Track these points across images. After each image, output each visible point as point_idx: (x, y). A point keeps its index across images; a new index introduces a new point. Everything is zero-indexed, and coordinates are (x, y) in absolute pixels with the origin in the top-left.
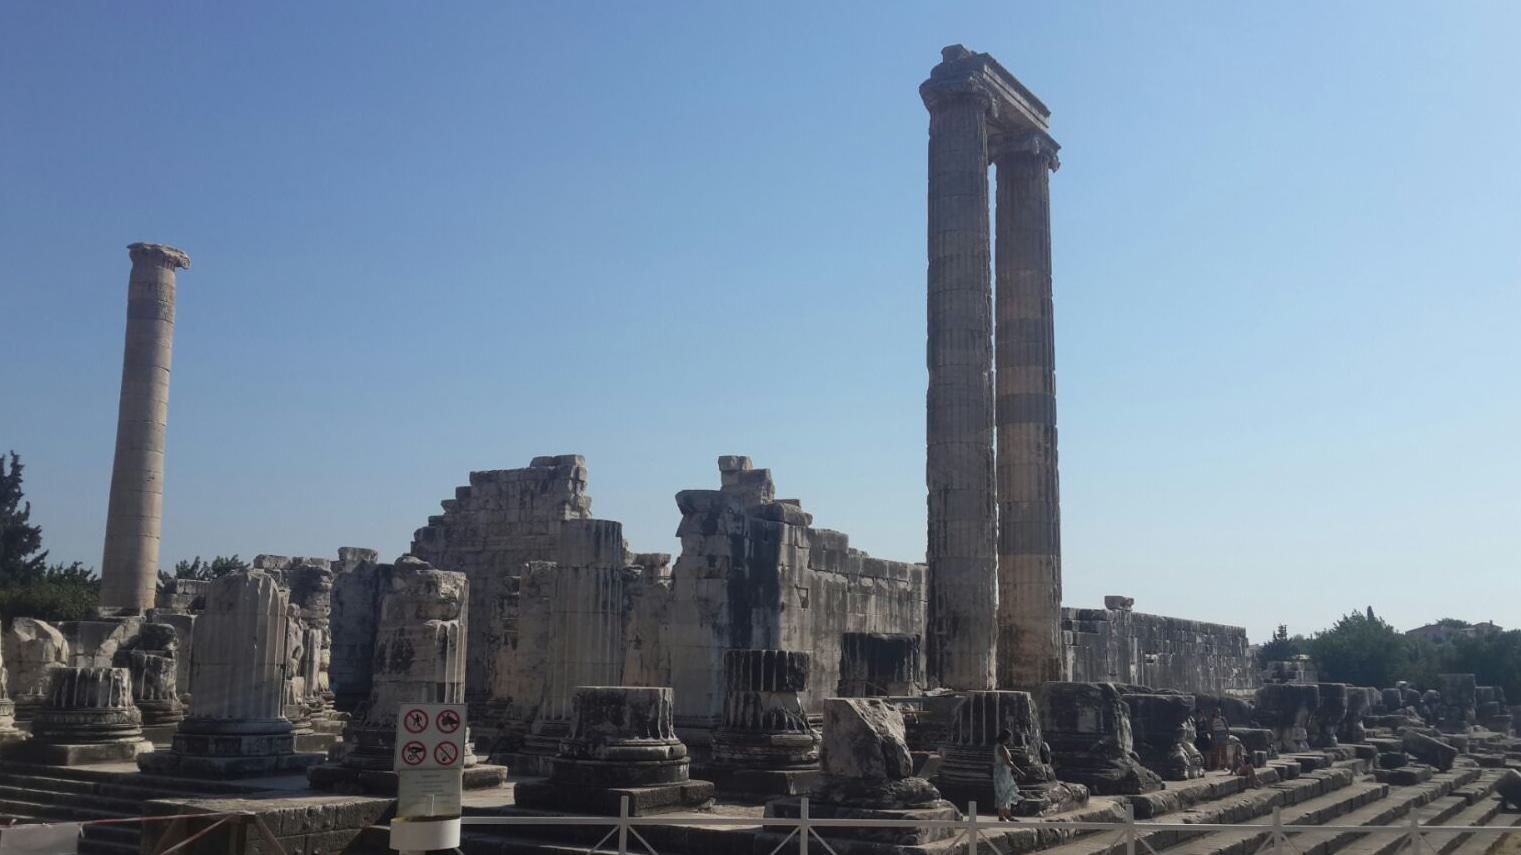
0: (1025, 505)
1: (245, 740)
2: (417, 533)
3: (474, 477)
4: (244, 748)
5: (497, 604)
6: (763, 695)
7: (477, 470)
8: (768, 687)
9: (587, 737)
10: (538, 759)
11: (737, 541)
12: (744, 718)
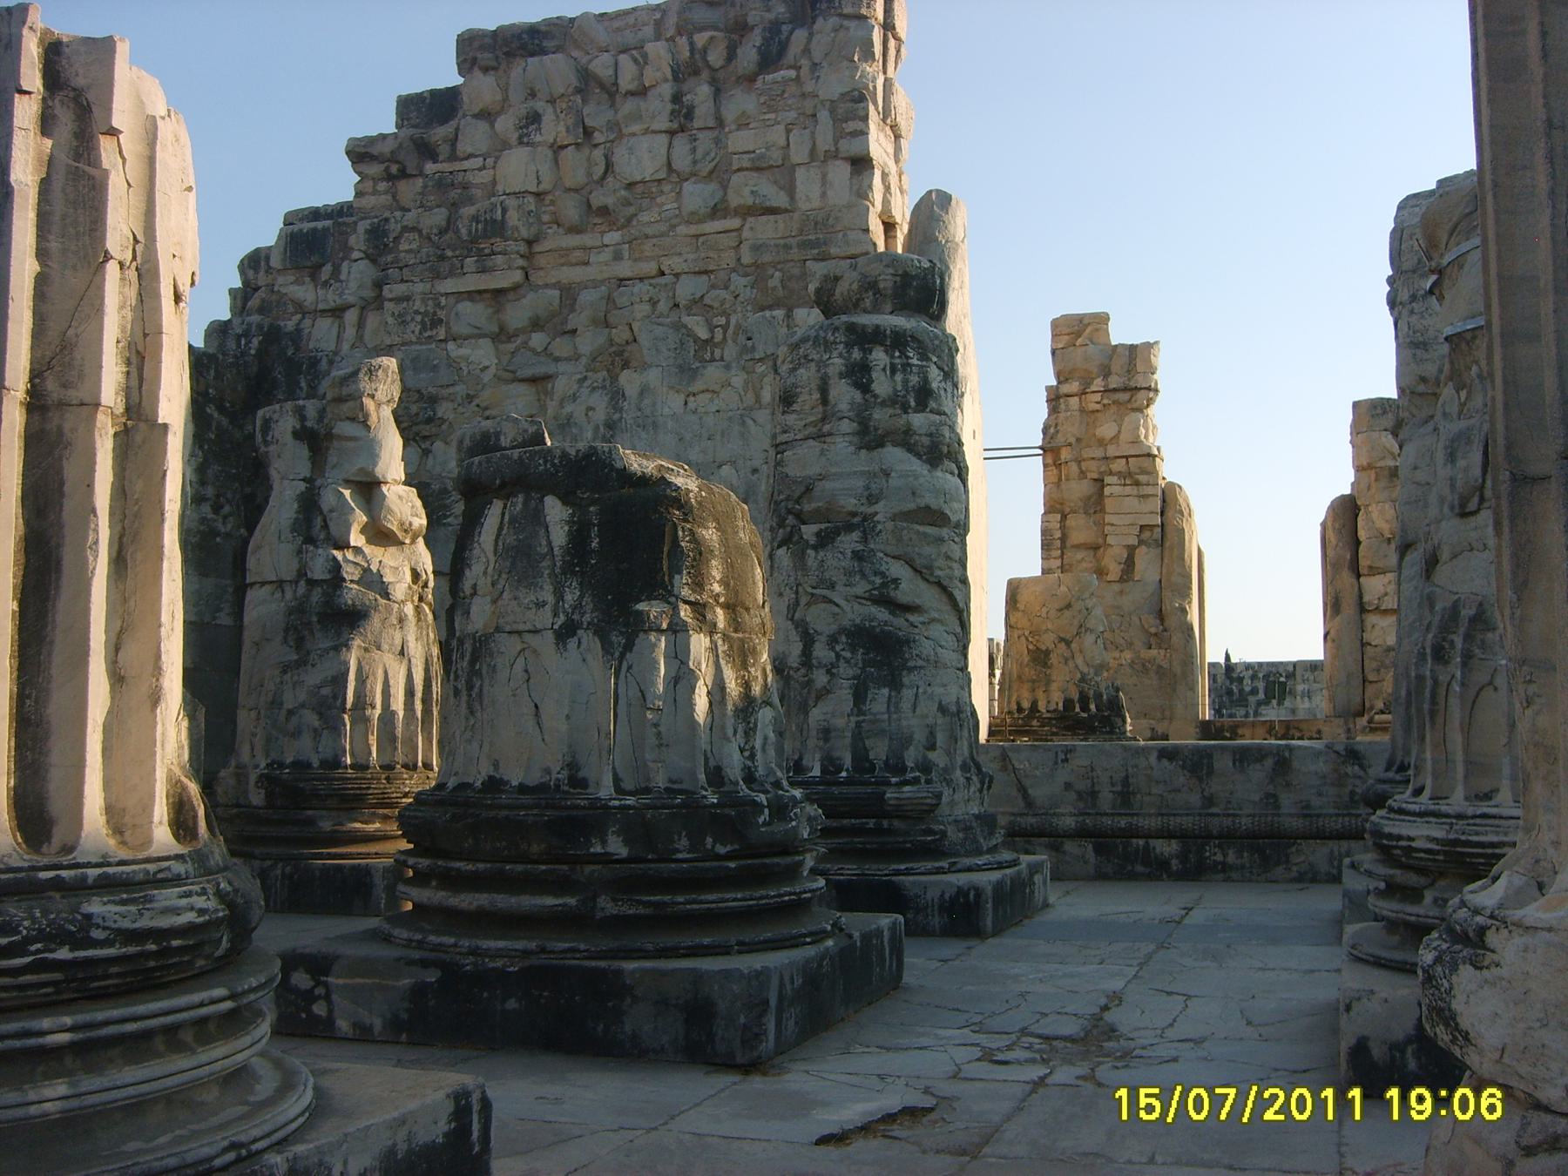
3: (477, 50)
5: (837, 363)
7: (489, 22)
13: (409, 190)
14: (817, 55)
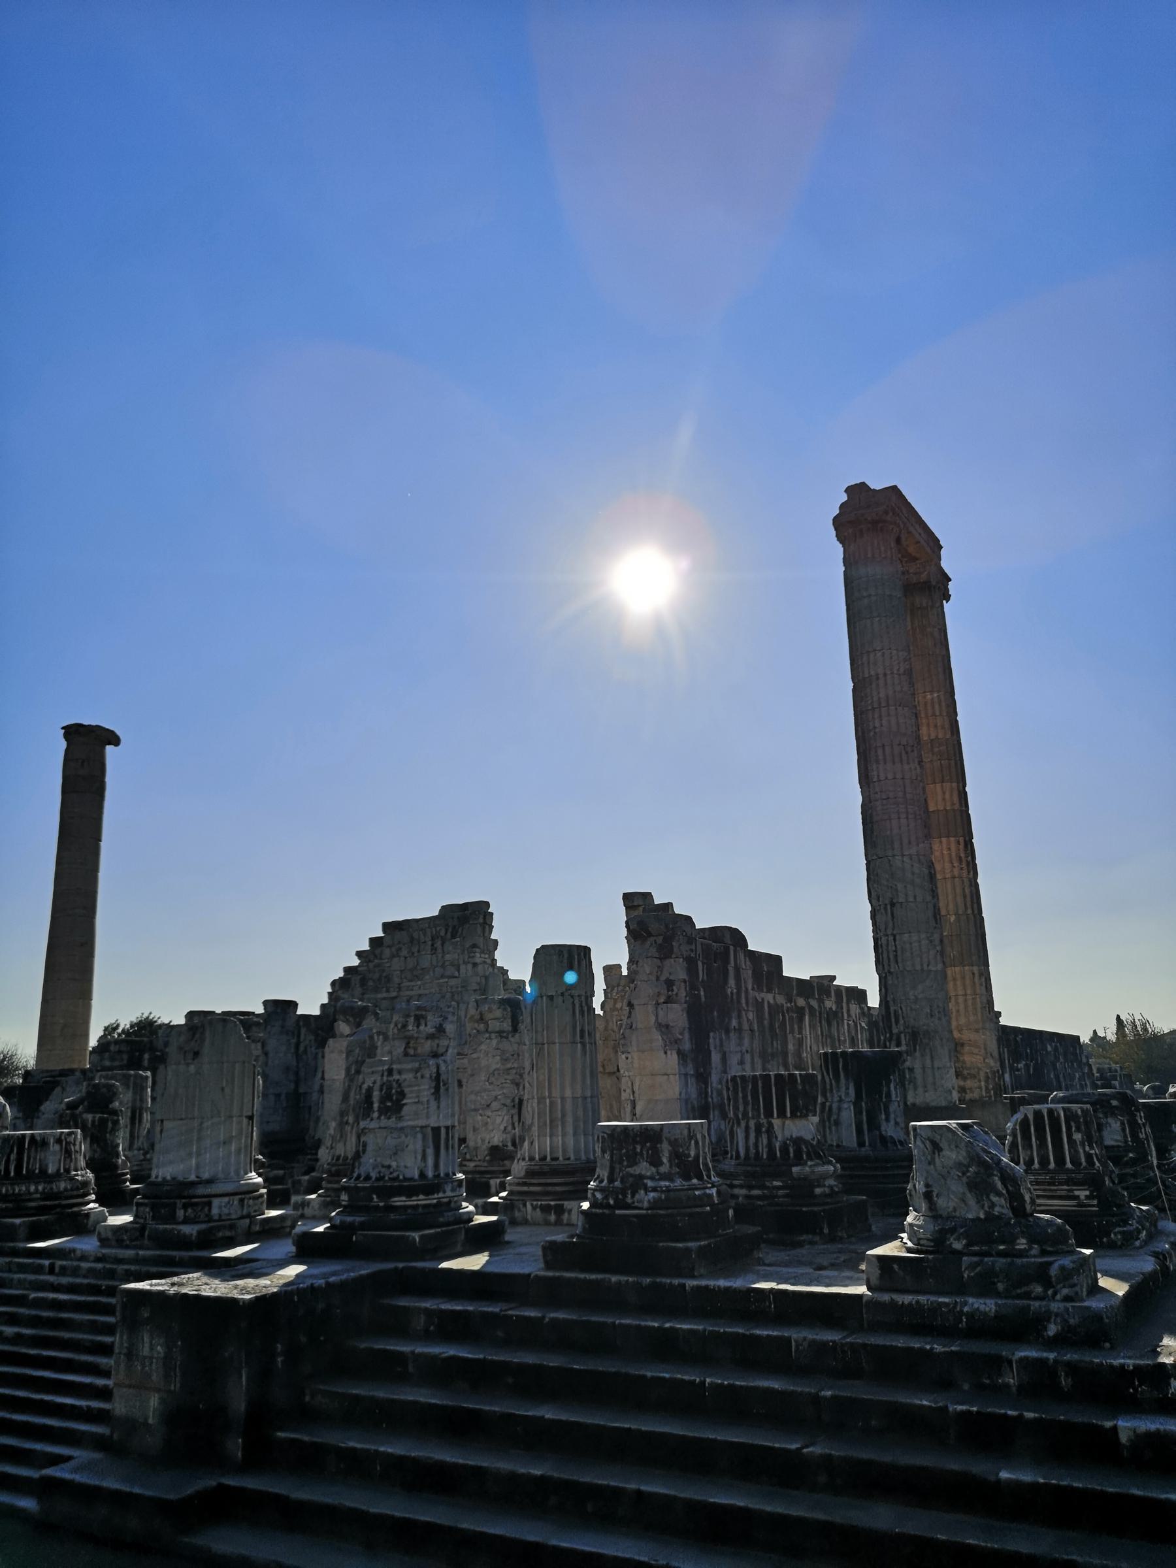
0: (953, 918)
1: (216, 1202)
2: (333, 984)
3: (386, 926)
4: (215, 1211)
6: (776, 1122)
8: (782, 1114)
9: (622, 1182)
10: (525, 1205)
11: (691, 963)
12: (757, 1153)
13: (371, 965)
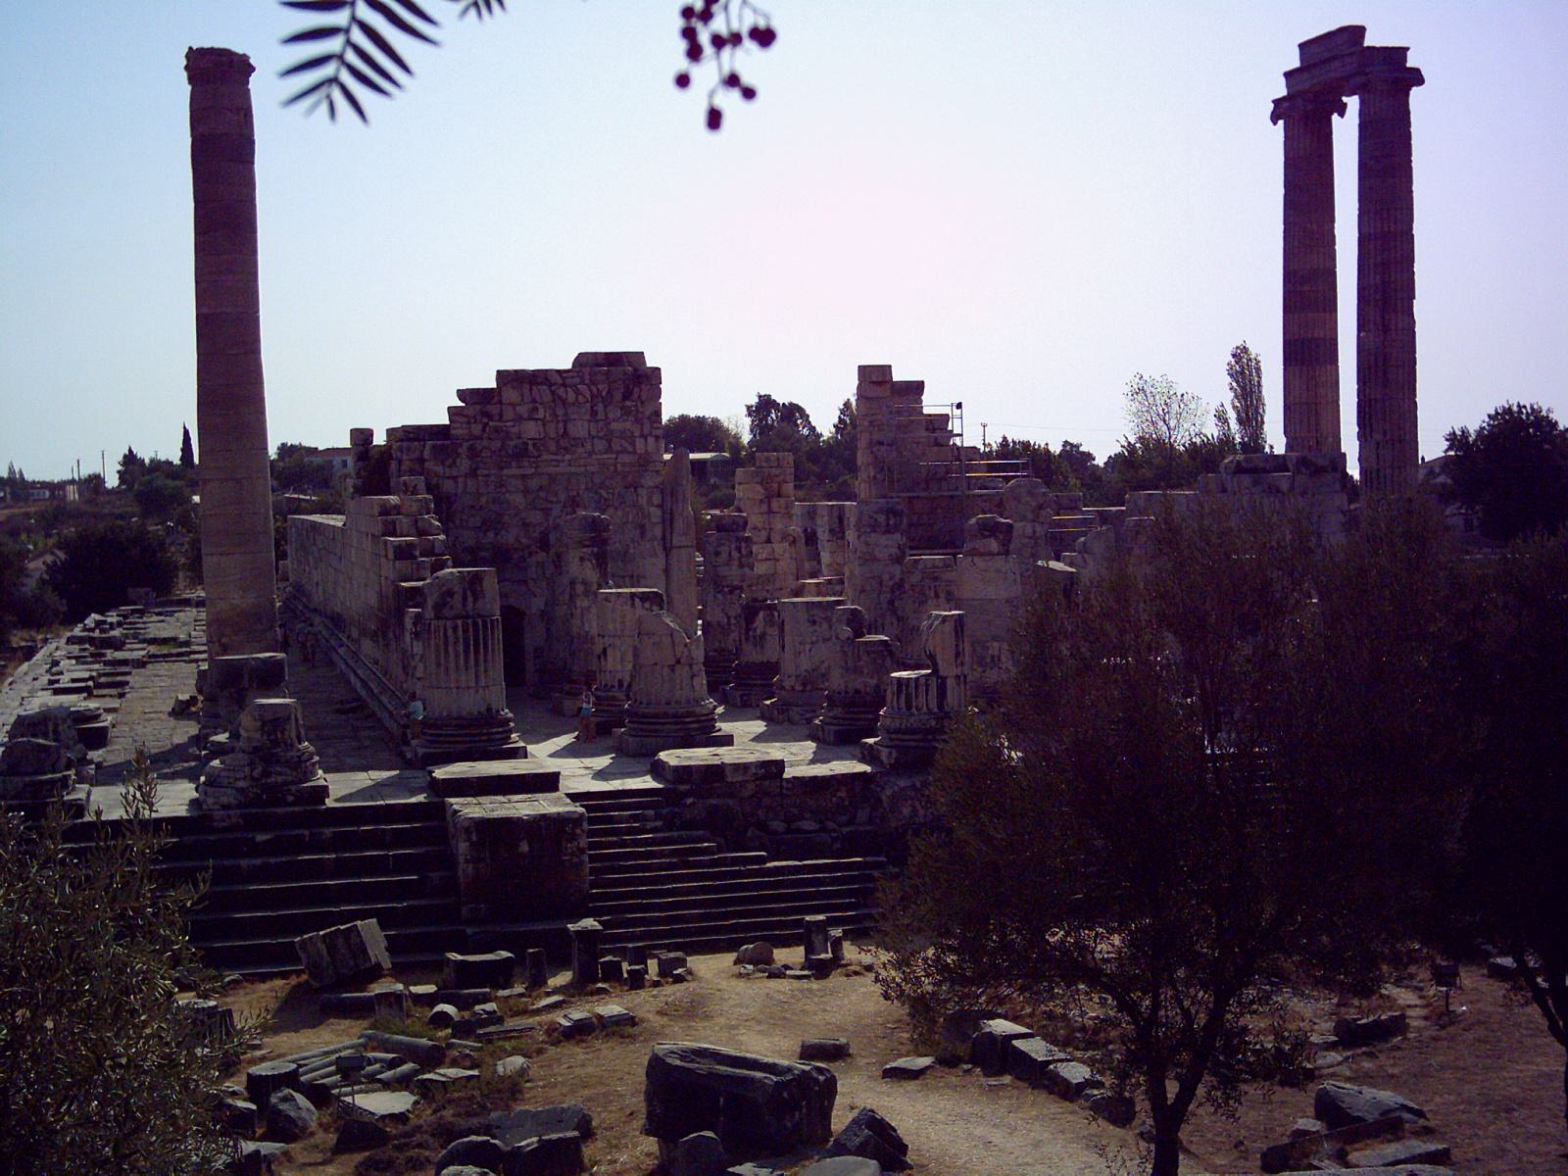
5: (733, 546)
14: (643, 398)
